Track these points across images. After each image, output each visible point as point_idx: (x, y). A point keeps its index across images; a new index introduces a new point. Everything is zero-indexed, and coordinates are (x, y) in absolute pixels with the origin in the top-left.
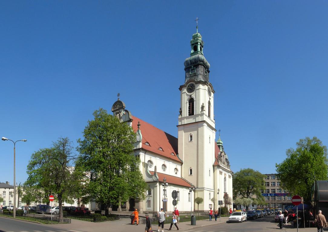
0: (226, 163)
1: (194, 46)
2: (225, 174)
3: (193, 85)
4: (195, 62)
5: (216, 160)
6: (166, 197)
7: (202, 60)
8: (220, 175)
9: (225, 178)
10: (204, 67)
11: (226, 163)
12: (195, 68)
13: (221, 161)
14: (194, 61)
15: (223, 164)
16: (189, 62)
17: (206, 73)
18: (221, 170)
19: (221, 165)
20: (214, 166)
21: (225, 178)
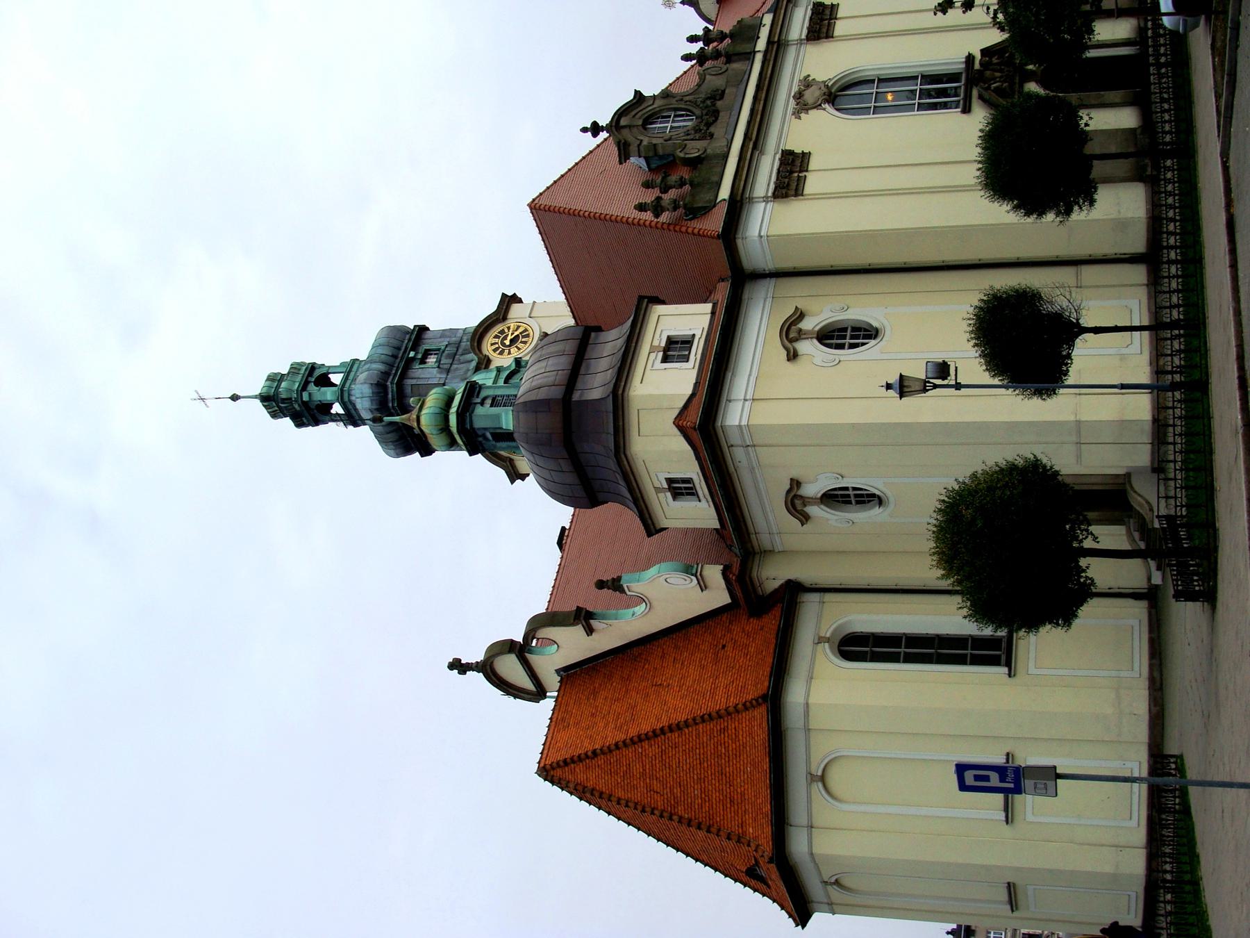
2: (802, 106)
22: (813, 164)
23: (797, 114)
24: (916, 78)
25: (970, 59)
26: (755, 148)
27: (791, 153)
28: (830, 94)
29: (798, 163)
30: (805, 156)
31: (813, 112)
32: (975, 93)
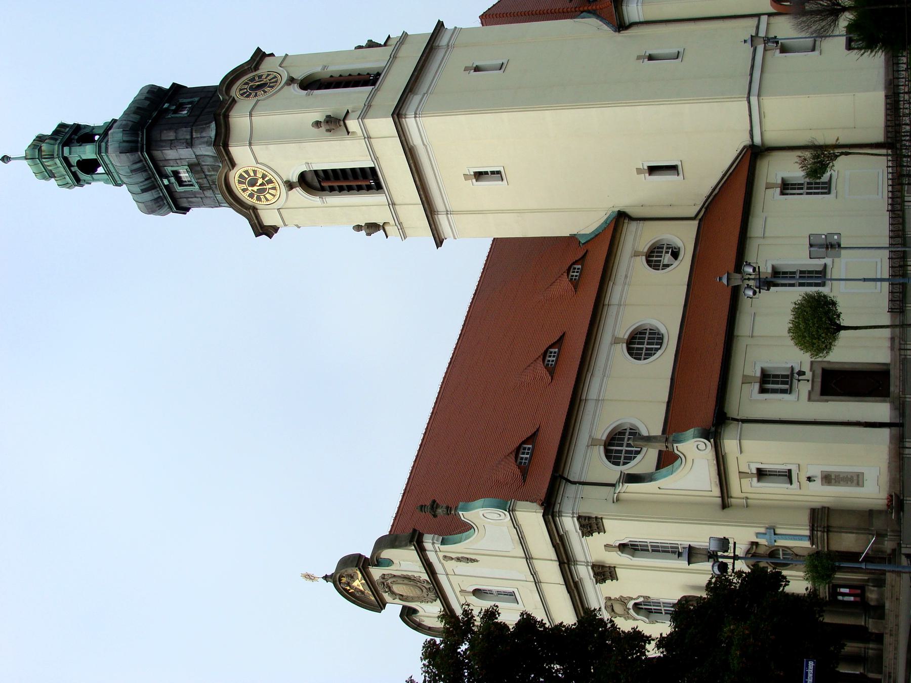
3: (241, 176)
4: (143, 169)
5: (589, 12)
6: (801, 378)
7: (125, 139)
10: (156, 121)
12: (169, 170)
14: (140, 177)
16: (148, 196)
17: (180, 107)
20: (621, 26)
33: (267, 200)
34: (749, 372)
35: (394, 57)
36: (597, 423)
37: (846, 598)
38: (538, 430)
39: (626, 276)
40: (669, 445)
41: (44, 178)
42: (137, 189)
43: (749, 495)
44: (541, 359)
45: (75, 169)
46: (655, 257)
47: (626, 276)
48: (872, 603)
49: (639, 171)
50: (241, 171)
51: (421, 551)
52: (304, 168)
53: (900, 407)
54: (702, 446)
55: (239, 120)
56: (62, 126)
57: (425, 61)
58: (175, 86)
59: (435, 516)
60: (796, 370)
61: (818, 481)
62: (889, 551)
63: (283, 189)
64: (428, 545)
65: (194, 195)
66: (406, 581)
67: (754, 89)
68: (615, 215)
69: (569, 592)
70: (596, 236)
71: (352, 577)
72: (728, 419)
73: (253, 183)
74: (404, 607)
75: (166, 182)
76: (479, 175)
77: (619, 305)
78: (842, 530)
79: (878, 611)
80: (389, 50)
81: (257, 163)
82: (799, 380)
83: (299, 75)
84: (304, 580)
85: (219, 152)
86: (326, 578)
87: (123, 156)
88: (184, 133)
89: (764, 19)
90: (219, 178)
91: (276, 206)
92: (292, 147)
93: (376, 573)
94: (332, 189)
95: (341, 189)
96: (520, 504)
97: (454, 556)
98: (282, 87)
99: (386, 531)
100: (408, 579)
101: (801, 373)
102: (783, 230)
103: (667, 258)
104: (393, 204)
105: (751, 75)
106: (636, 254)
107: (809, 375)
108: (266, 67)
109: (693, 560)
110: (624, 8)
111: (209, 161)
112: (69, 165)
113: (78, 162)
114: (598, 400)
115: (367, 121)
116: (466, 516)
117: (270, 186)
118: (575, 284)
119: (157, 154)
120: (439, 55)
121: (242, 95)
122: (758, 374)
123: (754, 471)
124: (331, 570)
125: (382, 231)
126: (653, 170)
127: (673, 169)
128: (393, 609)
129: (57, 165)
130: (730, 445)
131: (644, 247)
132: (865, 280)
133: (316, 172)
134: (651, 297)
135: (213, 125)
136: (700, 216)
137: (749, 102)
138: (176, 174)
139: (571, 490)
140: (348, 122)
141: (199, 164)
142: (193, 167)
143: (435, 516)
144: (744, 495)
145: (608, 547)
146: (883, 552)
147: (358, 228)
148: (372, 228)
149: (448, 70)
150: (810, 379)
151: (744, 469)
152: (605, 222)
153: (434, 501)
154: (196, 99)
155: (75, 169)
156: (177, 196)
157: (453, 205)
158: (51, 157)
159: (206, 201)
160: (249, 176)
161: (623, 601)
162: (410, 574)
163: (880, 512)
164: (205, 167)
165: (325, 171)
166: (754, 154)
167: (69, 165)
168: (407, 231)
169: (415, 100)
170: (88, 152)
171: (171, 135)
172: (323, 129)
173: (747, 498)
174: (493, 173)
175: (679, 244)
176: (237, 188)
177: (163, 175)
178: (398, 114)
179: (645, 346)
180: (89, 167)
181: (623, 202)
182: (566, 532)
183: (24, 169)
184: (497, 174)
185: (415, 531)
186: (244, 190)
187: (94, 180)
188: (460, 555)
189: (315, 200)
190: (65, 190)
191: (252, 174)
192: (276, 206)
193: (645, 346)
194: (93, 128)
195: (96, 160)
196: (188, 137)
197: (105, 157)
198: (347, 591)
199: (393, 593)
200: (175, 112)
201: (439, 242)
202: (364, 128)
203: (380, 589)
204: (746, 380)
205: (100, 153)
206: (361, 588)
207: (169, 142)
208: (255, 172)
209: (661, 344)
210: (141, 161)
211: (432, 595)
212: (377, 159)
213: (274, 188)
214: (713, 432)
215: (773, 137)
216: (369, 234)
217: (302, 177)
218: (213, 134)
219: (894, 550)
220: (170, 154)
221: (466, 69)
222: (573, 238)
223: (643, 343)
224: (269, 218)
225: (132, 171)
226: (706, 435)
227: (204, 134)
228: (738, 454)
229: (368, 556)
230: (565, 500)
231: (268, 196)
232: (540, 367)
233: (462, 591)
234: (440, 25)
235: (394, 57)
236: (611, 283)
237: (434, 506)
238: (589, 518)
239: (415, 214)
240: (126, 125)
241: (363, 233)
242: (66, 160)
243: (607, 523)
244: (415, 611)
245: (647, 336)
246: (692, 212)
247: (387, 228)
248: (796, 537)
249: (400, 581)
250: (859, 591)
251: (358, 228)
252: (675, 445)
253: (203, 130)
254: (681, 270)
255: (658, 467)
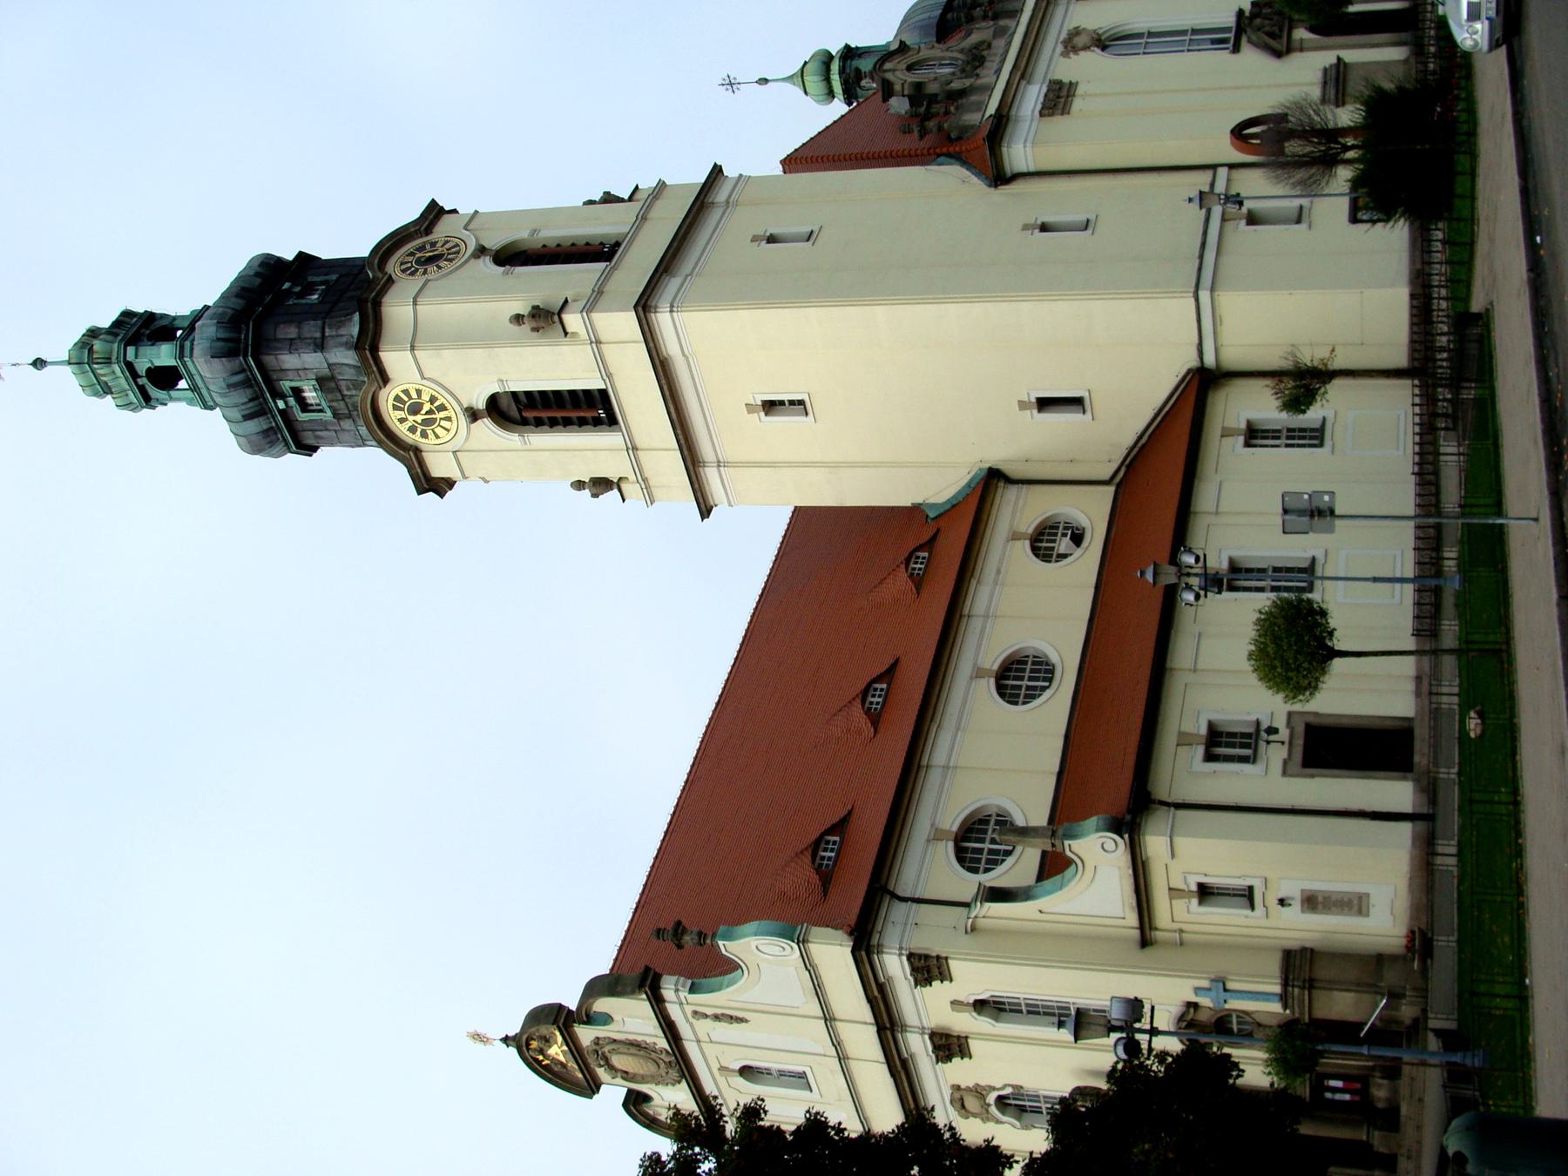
0: (975, 38)
1: (154, 392)
2: (1071, 45)
3: (397, 398)
4: (248, 383)
5: (949, 155)
6: (1272, 738)
7: (222, 335)
8: (1077, 104)
9: (1102, 42)
11: (975, 38)
12: (286, 385)
13: (962, 93)
14: (241, 396)
15: (986, 76)
16: (253, 426)
17: (309, 289)
18: (1032, 96)
19: (992, 108)
20: (999, 177)
21: (1102, 42)
22: (1080, 90)
23: (1065, 54)
24: (1184, 33)
25: (1240, 13)
26: (1022, 77)
27: (1059, 83)
28: (1099, 40)
29: (1064, 93)
30: (1072, 86)
31: (1082, 54)
32: (1244, 39)
33: (437, 437)
34: (1188, 727)
35: (642, 218)
36: (945, 803)
37: (1338, 1096)
38: (850, 812)
39: (998, 572)
40: (1058, 843)
41: (96, 394)
42: (237, 415)
43: (1184, 927)
44: (859, 700)
45: (143, 381)
46: (1045, 541)
47: (998, 572)
48: (1380, 1105)
49: (1023, 405)
50: (397, 391)
51: (657, 1002)
52: (496, 389)
53: (1430, 789)
54: (1110, 845)
55: (397, 310)
56: (127, 314)
57: (691, 225)
58: (302, 257)
59: (680, 946)
60: (1264, 726)
61: (1296, 905)
62: (1408, 1022)
63: (463, 420)
64: (668, 992)
65: (324, 426)
66: (633, 1050)
67: (1205, 277)
68: (983, 474)
69: (893, 1075)
70: (953, 508)
71: (547, 1041)
72: (1154, 802)
73: (415, 409)
74: (630, 1092)
75: (281, 404)
76: (770, 406)
77: (986, 616)
78: (1332, 985)
79: (1389, 1119)
80: (635, 207)
81: (423, 377)
82: (1268, 742)
83: (494, 241)
84: (470, 1042)
85: (363, 359)
86: (506, 1040)
87: (217, 363)
88: (311, 329)
89: (1223, 172)
90: (363, 400)
91: (449, 447)
92: (478, 354)
93: (586, 1035)
94: (539, 423)
95: (553, 423)
96: (816, 931)
97: (709, 1011)
98: (466, 262)
99: (604, 967)
100: (636, 1046)
101: (1272, 730)
102: (1242, 506)
103: (1064, 544)
104: (635, 448)
105: (1201, 257)
106: (1015, 536)
107: (1284, 734)
108: (442, 230)
109: (1083, 1033)
110: (1004, 150)
111: (349, 374)
112: (134, 375)
113: (149, 370)
114: (946, 767)
115: (595, 316)
116: (729, 948)
117: (443, 414)
118: (918, 582)
119: (269, 360)
120: (713, 217)
121: (404, 271)
122: (1203, 731)
123: (1194, 888)
124: (514, 1028)
125: (616, 491)
126: (1044, 404)
127: (1076, 403)
128: (613, 1093)
129: (116, 374)
130: (1155, 844)
131: (1028, 524)
132: (1375, 580)
133: (514, 394)
134: (1037, 605)
135: (356, 317)
136: (1117, 479)
137: (1197, 300)
138: (297, 392)
139: (900, 909)
140: (565, 317)
141: (332, 378)
142: (325, 383)
143: (680, 946)
144: (1176, 926)
145: (956, 1004)
146: (1397, 1022)
147: (579, 485)
148: (601, 485)
149: (725, 240)
150: (1286, 739)
151: (1177, 883)
152: (968, 485)
153: (679, 923)
154: (334, 277)
155: (143, 381)
156: (299, 427)
157: (728, 453)
158: (108, 361)
159: (345, 437)
160: (410, 398)
161: (979, 1092)
162: (640, 1038)
163: (1394, 958)
164: (343, 385)
165: (528, 394)
166: (1203, 383)
167: (134, 375)
168: (655, 492)
169: (672, 285)
170: (163, 355)
171: (291, 332)
172: (526, 327)
173: (1181, 931)
174: (792, 403)
175: (1083, 521)
176: (392, 417)
177: (278, 394)
178: (644, 306)
179: (1025, 683)
180: (166, 378)
181: (997, 454)
182: (889, 979)
183: (66, 380)
184: (799, 405)
185: (647, 969)
186: (402, 421)
187: (171, 399)
188: (719, 1011)
189: (512, 439)
190: (127, 413)
191: (414, 395)
192: (449, 447)
193: (1025, 683)
194: (175, 318)
195: (173, 369)
196: (318, 335)
197: (189, 364)
198: (539, 1062)
199: (611, 1068)
200: (301, 295)
201: (705, 511)
202: (591, 327)
203: (591, 1060)
204: (1184, 740)
205: (181, 356)
206: (562, 1058)
207: (288, 343)
208: (419, 392)
209: (1050, 680)
210: (243, 371)
211: (674, 1074)
212: (609, 376)
213: (448, 419)
214: (1129, 822)
215: (1235, 355)
216: (595, 495)
217: (493, 400)
218: (355, 331)
219: (1416, 1021)
220: (289, 361)
221: (755, 239)
222: (915, 511)
223: (1022, 679)
224: (439, 466)
225: (229, 386)
226: (1116, 827)
227: (342, 331)
228: (1169, 860)
229: (573, 1007)
230: (889, 926)
231: (439, 431)
232: (857, 711)
233: (722, 1069)
234: (717, 171)
235: (642, 218)
236: (974, 582)
237: (679, 930)
238: (927, 957)
239: (667, 465)
240: (223, 314)
241: (587, 493)
242: (130, 366)
243: (955, 966)
244: (646, 1098)
245: (1029, 667)
246: (1105, 472)
247: (624, 486)
248: (1259, 996)
249: (623, 1049)
250: (1358, 1086)
251: (579, 485)
252: (1067, 843)
253: (341, 325)
254: (1084, 565)
255: (1041, 877)
